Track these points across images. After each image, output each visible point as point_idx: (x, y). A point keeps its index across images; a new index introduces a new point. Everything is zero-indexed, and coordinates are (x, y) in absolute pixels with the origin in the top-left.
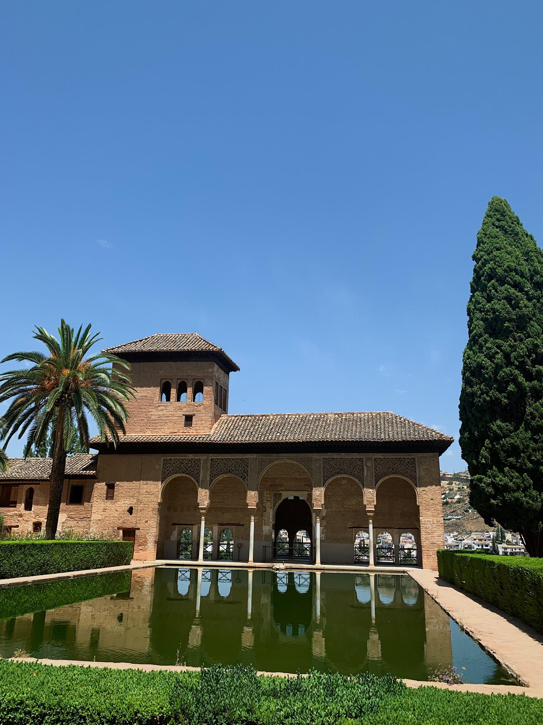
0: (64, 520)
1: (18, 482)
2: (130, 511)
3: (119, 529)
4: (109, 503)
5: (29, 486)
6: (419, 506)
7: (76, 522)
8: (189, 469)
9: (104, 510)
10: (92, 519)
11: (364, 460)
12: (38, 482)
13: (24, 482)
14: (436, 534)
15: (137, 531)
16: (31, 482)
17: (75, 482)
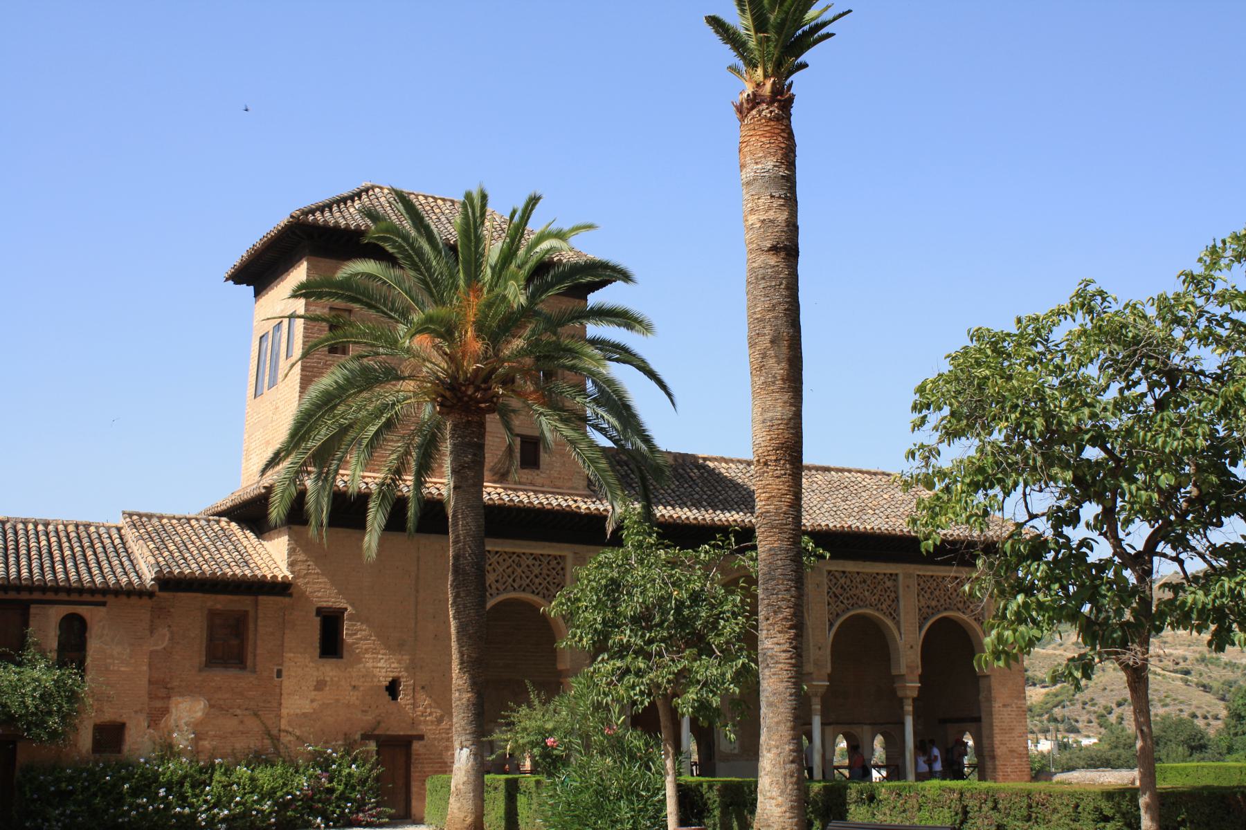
0: (199, 714)
1: (25, 596)
2: (393, 689)
3: (366, 737)
4: (329, 669)
5: (65, 610)
6: (988, 676)
7: (235, 721)
8: (537, 581)
9: (320, 686)
10: (284, 711)
11: (901, 578)
12: (98, 598)
13: (50, 596)
14: (1016, 734)
15: (416, 745)
16: (75, 597)
17: (221, 602)
